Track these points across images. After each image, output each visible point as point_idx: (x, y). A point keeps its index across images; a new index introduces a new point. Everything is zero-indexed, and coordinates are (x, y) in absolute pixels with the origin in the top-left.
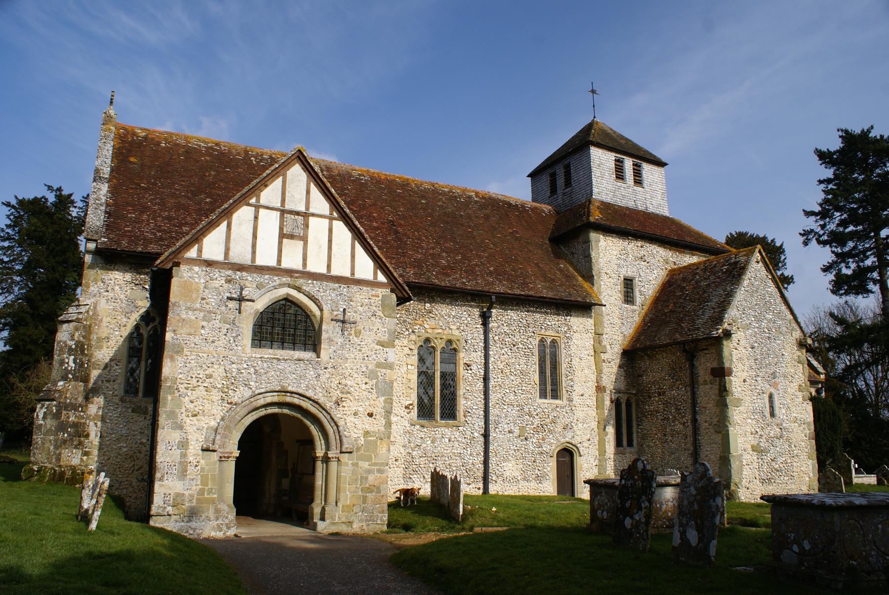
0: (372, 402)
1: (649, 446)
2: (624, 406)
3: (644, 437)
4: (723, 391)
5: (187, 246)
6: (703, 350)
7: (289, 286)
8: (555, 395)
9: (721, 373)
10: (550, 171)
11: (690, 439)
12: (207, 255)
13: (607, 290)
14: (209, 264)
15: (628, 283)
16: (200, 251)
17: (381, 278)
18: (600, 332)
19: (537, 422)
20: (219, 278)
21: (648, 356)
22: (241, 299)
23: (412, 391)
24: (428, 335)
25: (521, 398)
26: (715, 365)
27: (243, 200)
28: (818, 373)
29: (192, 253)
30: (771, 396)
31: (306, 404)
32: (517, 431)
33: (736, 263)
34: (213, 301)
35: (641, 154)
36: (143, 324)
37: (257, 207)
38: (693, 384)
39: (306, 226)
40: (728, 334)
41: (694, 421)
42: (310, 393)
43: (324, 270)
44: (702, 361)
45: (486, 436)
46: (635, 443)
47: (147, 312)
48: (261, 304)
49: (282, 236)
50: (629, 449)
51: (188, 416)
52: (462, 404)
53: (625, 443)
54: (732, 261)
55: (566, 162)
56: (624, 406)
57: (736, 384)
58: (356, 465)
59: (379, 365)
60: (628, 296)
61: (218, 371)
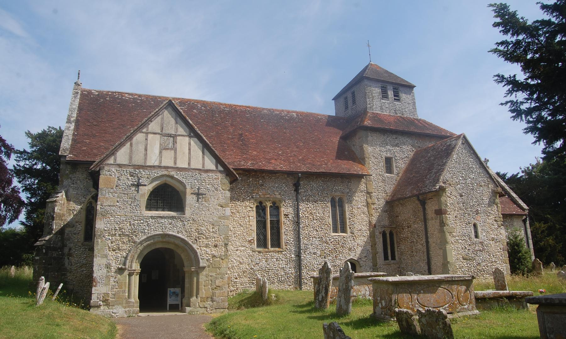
0: (216, 239)
1: (404, 259)
2: (388, 235)
3: (402, 253)
4: (442, 224)
5: (108, 157)
6: (430, 199)
8: (344, 230)
9: (440, 212)
10: (345, 96)
11: (425, 253)
12: (118, 162)
13: (373, 166)
14: (120, 166)
15: (388, 161)
16: (115, 160)
17: (220, 168)
18: (370, 191)
19: (332, 247)
21: (401, 204)
22: (138, 185)
23: (252, 232)
24: (261, 199)
25: (321, 234)
26: (437, 208)
27: (138, 130)
28: (524, 210)
29: (111, 161)
30: (475, 226)
32: (319, 253)
33: (450, 145)
35: (398, 82)
37: (147, 133)
38: (425, 220)
39: (175, 142)
40: (442, 189)
41: (427, 242)
43: (186, 166)
44: (430, 205)
45: (298, 256)
46: (397, 258)
48: (150, 187)
50: (392, 261)
51: (109, 251)
52: (284, 238)
53: (390, 258)
54: (448, 144)
55: (352, 90)
56: (388, 235)
57: (450, 218)
59: (220, 218)
60: (389, 169)
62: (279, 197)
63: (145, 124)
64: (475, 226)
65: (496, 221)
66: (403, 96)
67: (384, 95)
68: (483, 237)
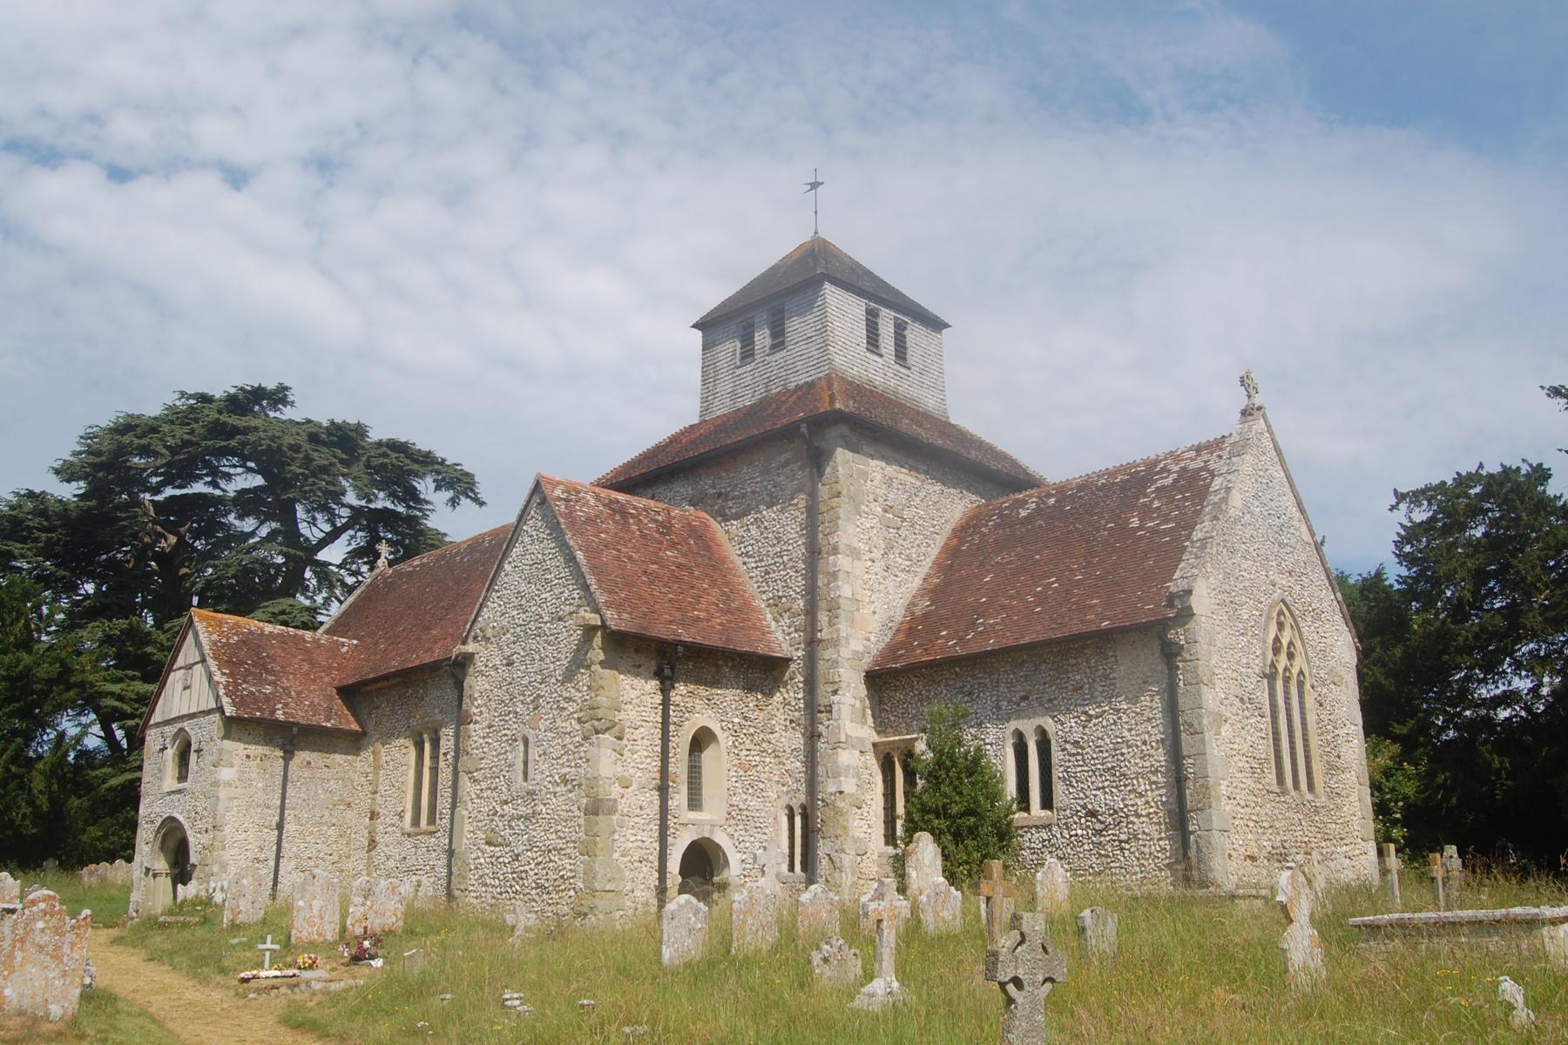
14: (157, 725)
30: (526, 742)
62: (439, 717)
64: (526, 742)
65: (579, 720)
66: (796, 326)
67: (748, 354)
68: (538, 777)
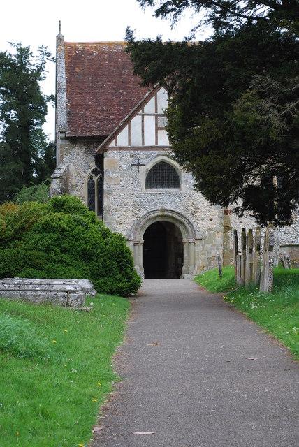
5: (110, 141)
7: (163, 155)
12: (119, 145)
14: (121, 148)
16: (116, 142)
20: (127, 154)
22: (138, 165)
27: (135, 113)
29: (112, 144)
31: (177, 217)
34: (125, 168)
36: (94, 175)
37: (143, 116)
42: (177, 210)
47: (96, 169)
48: (149, 166)
49: (157, 129)
58: (204, 246)
61: (130, 202)
63: (141, 107)
